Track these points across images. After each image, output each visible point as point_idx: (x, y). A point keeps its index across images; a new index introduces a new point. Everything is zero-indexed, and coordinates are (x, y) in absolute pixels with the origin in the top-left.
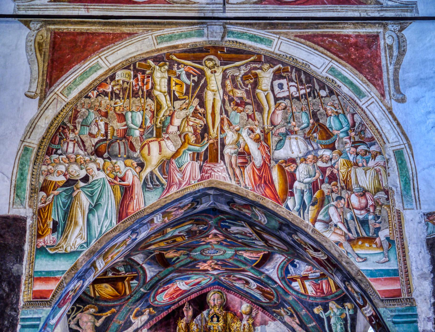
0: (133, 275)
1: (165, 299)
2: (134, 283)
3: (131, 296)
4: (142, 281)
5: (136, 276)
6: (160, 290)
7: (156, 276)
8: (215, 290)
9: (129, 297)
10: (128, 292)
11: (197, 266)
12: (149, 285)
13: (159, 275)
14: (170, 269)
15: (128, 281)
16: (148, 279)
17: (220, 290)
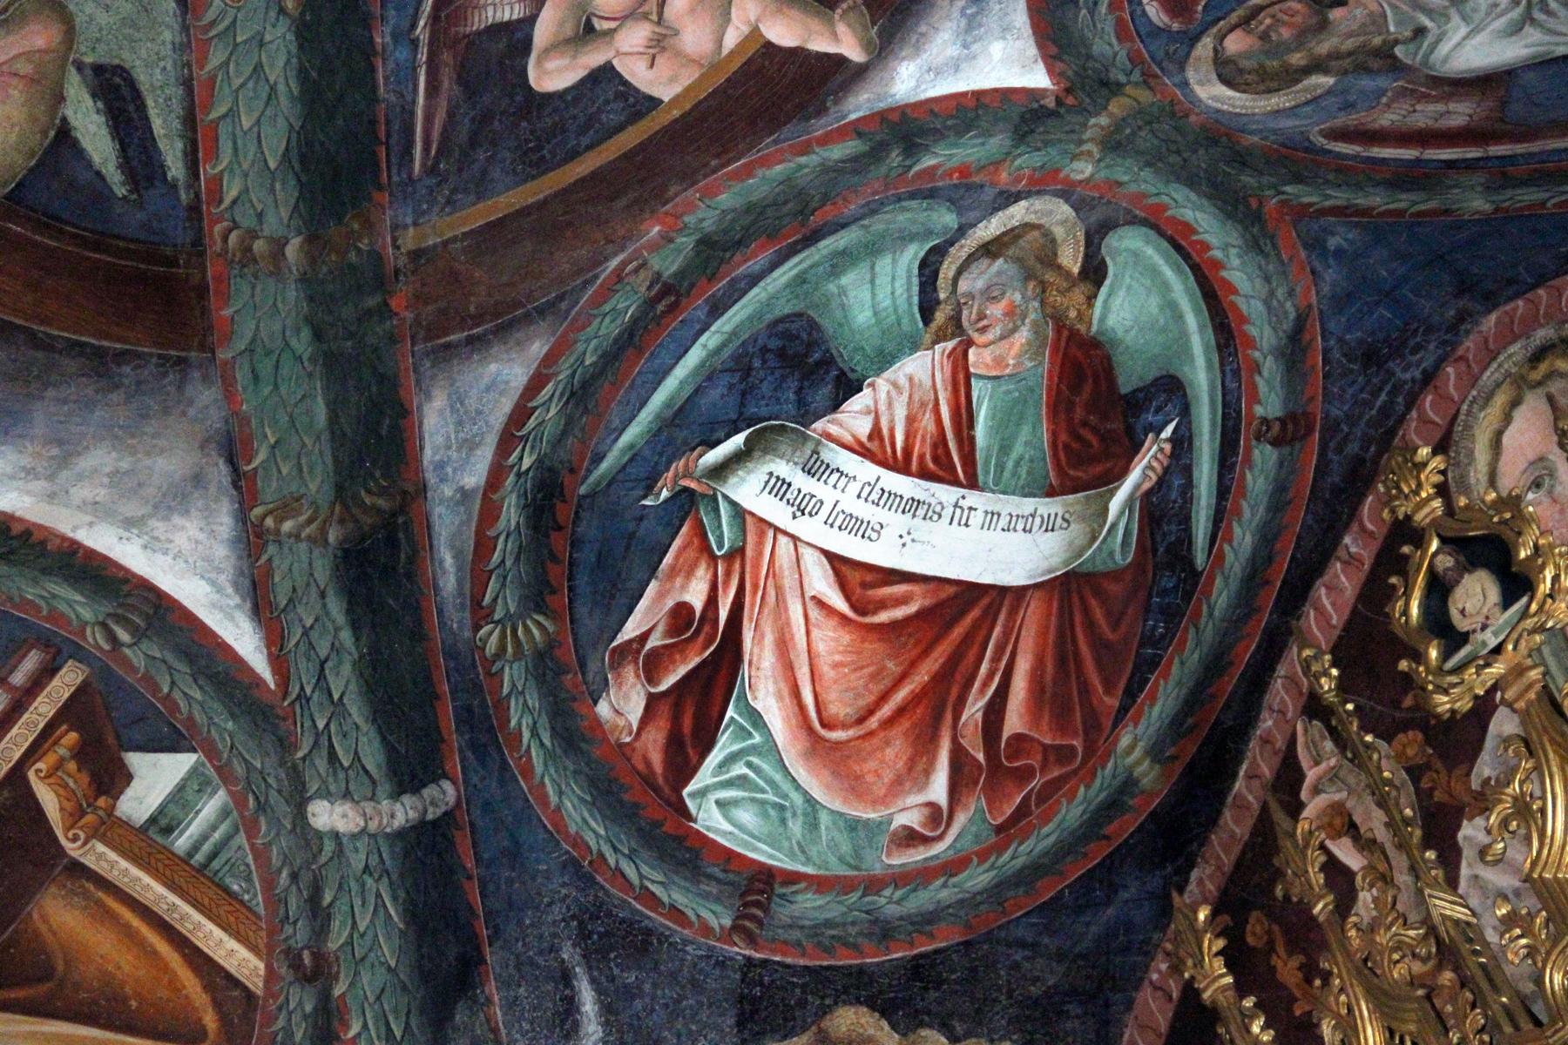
0: (43, 708)
1: (909, 816)
2: (181, 800)
3: (317, 973)
4: (226, 727)
5: (82, 691)
6: (624, 705)
7: (253, 540)
8: (1489, 377)
9: (303, 1000)
10: (238, 958)
11: (552, 75)
12: (338, 708)
13: (270, 491)
14: (262, 314)
15: (113, 830)
16: (244, 639)
17: (1542, 334)
